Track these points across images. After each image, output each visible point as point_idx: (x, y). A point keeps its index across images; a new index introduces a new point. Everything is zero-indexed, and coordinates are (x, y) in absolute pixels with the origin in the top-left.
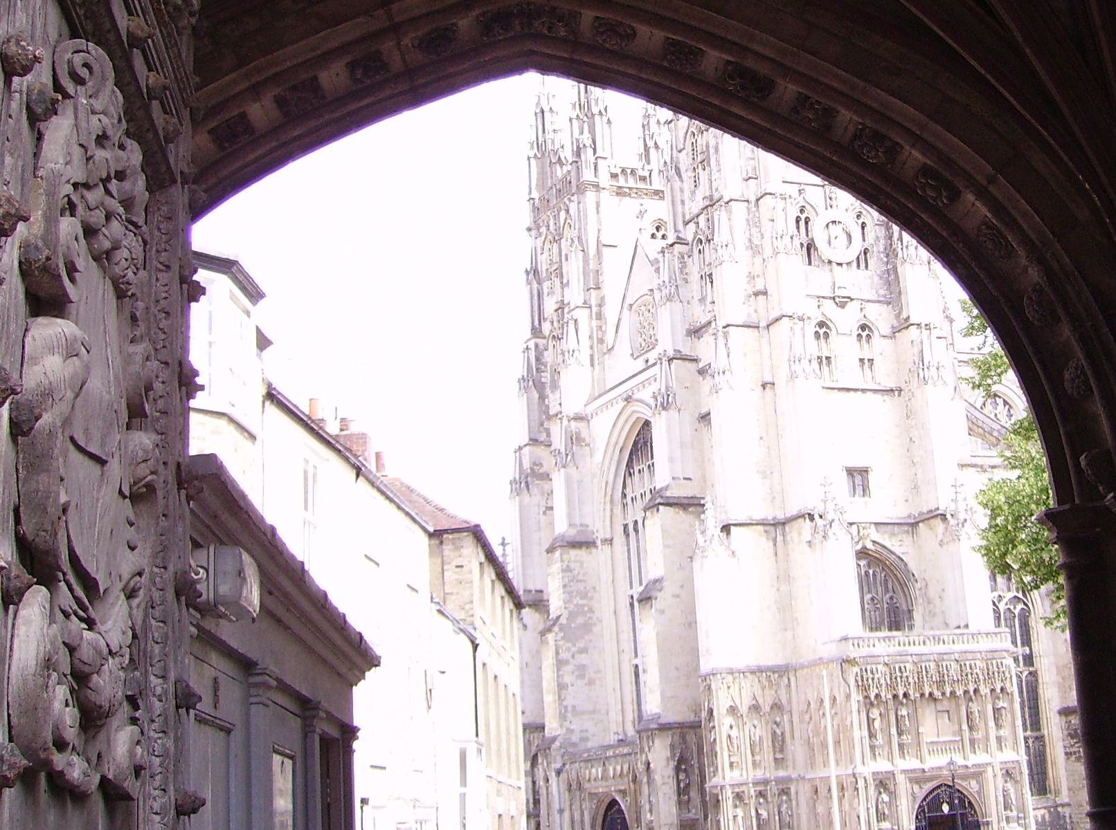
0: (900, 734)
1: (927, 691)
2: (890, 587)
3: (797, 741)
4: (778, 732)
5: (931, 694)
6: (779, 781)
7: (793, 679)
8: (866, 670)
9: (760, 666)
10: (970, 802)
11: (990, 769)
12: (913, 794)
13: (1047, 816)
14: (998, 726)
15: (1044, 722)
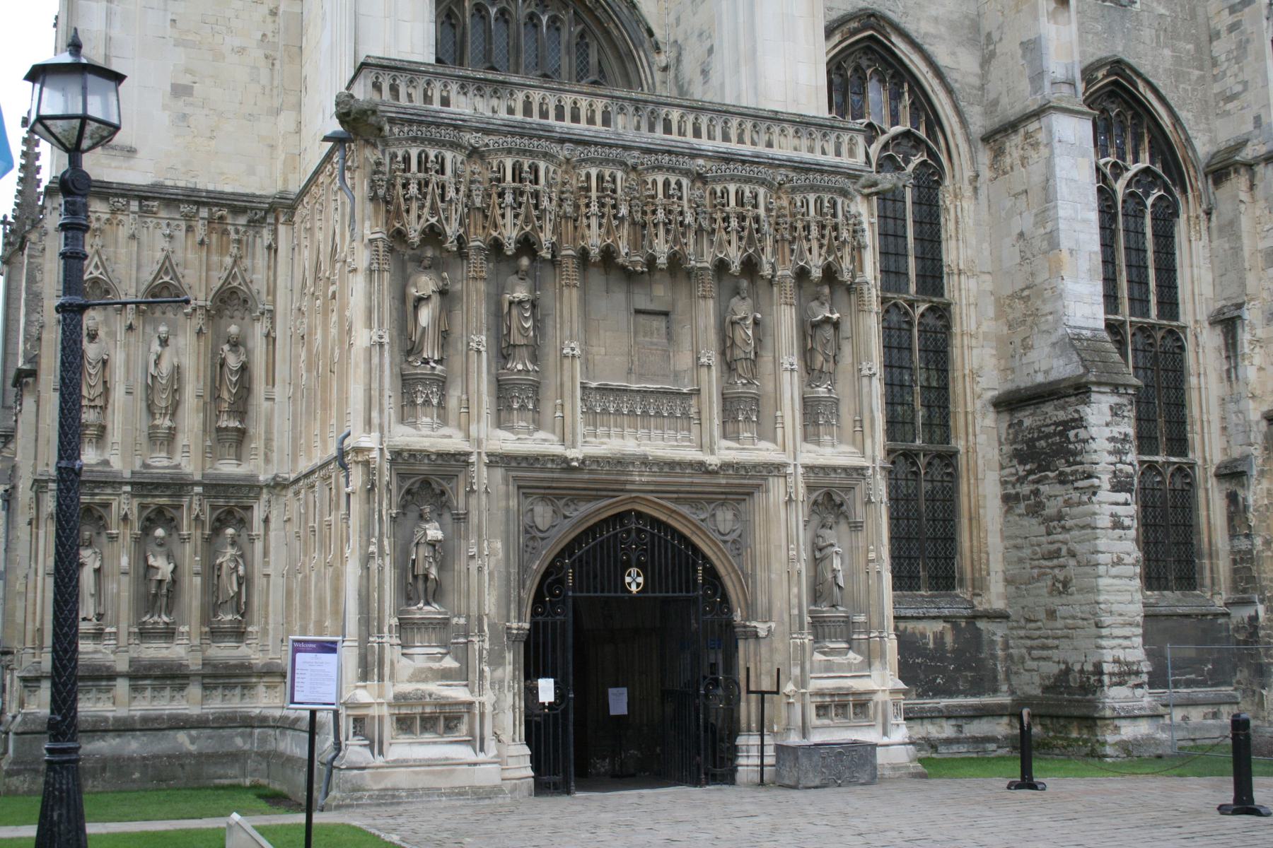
0: (504, 353)
1: (594, 239)
2: (593, 59)
3: (279, 392)
4: (233, 362)
5: (608, 254)
6: (215, 487)
7: (282, 229)
8: (407, 160)
9: (193, 190)
10: (712, 575)
11: (777, 490)
12: (531, 533)
13: (949, 639)
14: (811, 373)
15: (958, 422)
